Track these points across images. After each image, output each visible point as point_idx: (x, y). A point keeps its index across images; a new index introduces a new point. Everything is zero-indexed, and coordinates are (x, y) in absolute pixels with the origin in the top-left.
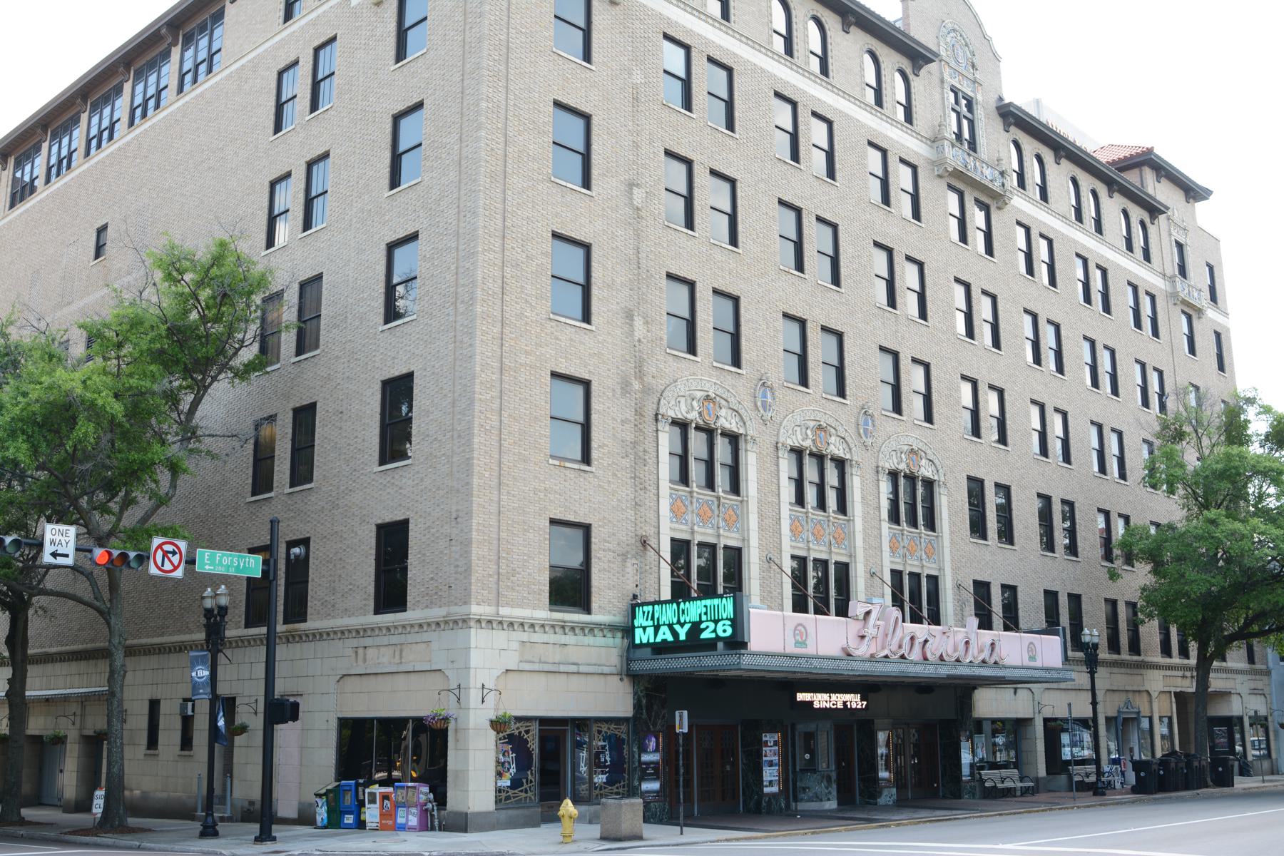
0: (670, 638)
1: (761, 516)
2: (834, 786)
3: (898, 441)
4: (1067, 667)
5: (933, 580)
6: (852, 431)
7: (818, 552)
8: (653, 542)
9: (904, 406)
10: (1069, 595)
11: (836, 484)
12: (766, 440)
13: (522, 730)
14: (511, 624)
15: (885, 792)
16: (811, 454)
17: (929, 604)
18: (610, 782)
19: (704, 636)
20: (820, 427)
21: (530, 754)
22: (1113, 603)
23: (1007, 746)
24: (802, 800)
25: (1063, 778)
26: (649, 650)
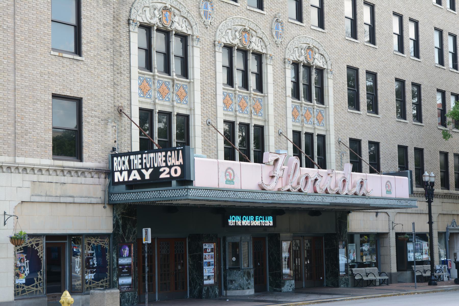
0: (139, 178)
1: (203, 93)
2: (252, 279)
3: (299, 40)
4: (413, 198)
5: (322, 138)
6: (267, 33)
7: (242, 118)
8: (126, 111)
9: (304, 16)
10: (415, 149)
11: (256, 70)
12: (207, 40)
13: (34, 243)
14: (25, 169)
15: (287, 283)
16: (239, 50)
17: (318, 154)
18: (97, 279)
19: (162, 176)
20: (245, 31)
21: (39, 260)
22: (445, 155)
23: (371, 252)
24: (230, 289)
25: (408, 274)
26: (124, 186)
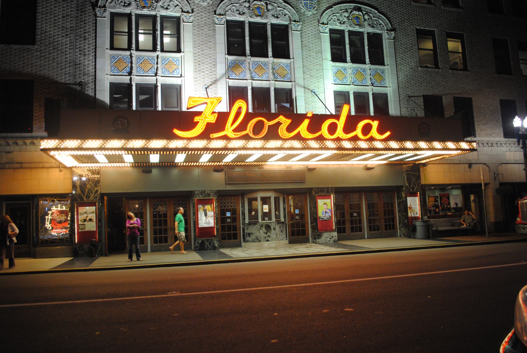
24: (248, 241)
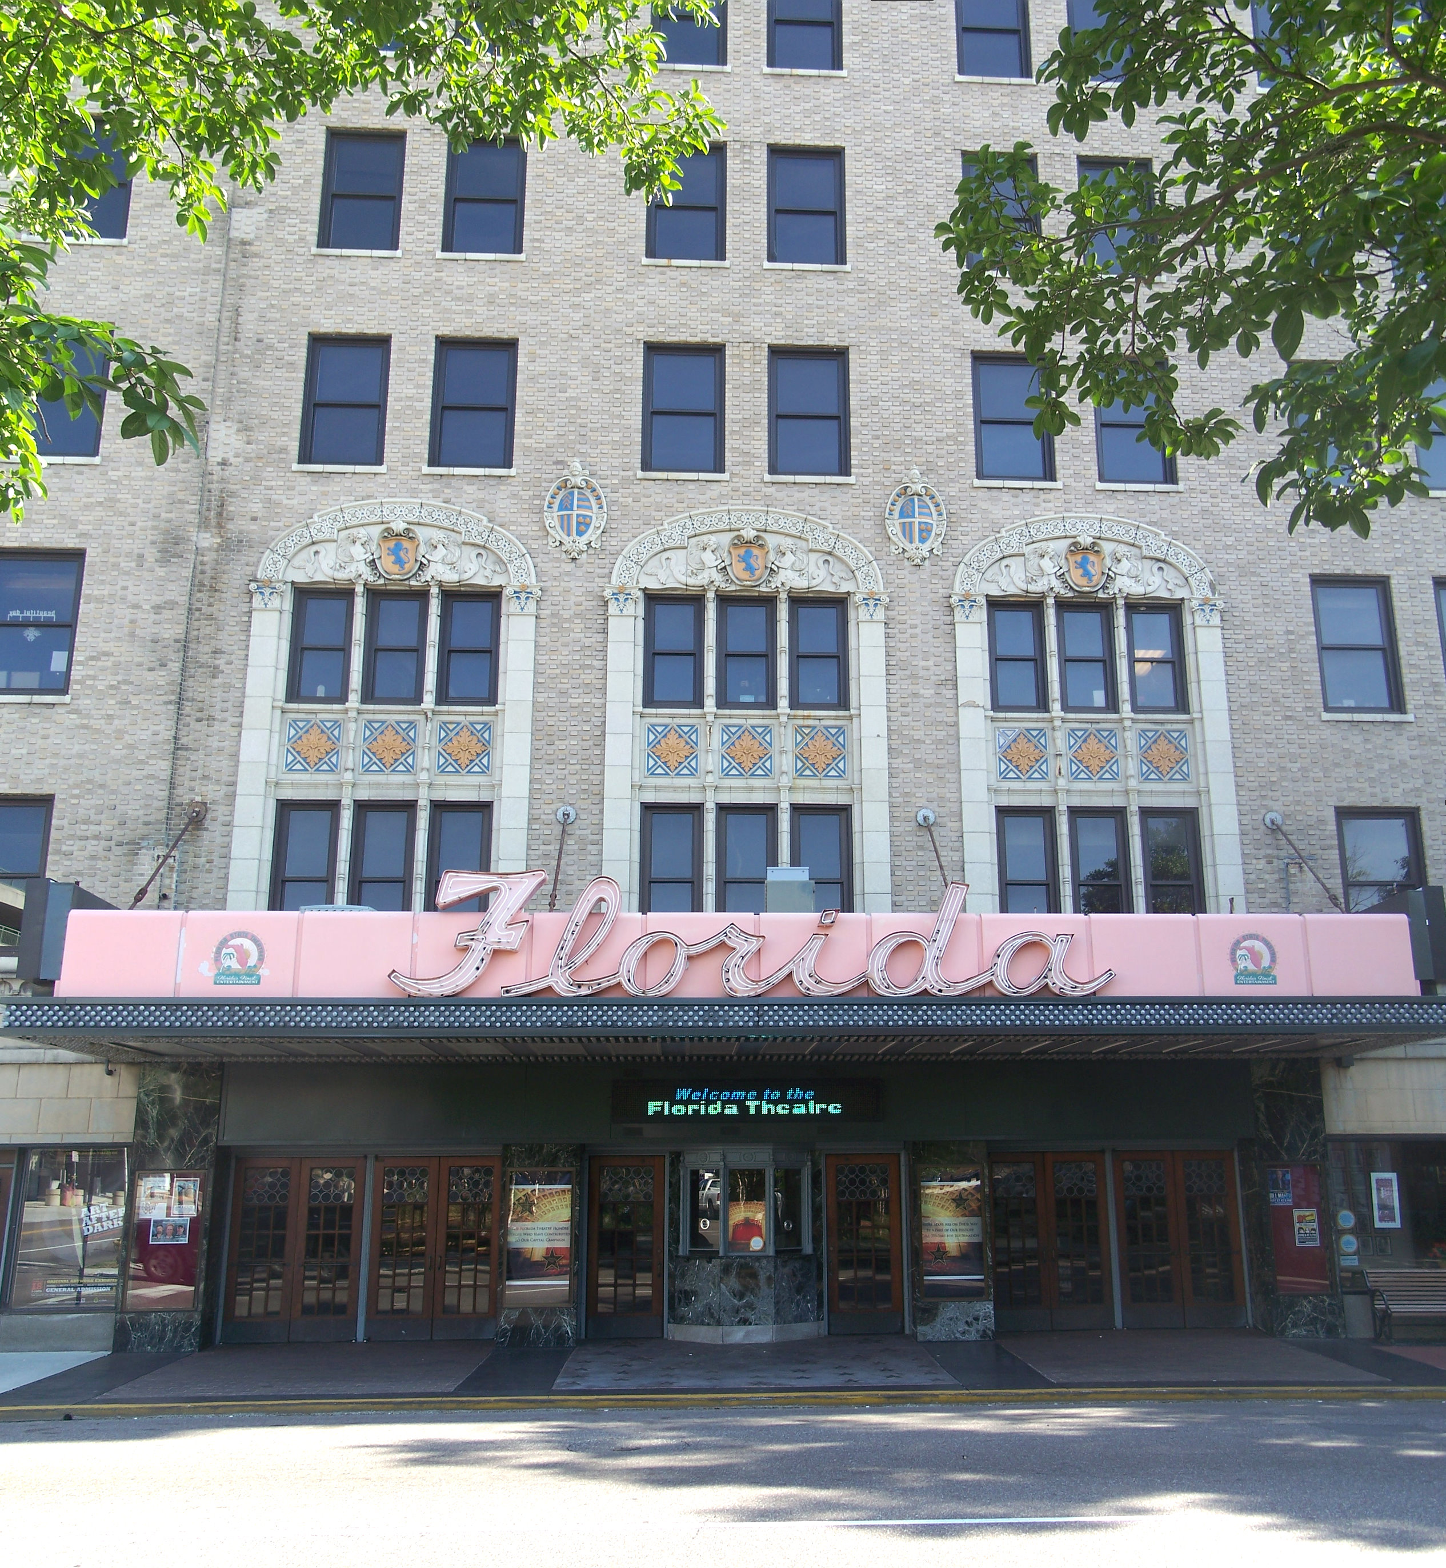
8: (219, 812)
